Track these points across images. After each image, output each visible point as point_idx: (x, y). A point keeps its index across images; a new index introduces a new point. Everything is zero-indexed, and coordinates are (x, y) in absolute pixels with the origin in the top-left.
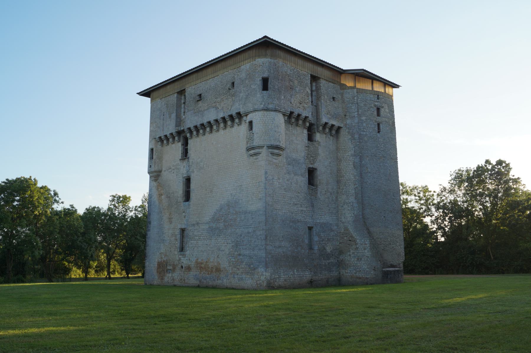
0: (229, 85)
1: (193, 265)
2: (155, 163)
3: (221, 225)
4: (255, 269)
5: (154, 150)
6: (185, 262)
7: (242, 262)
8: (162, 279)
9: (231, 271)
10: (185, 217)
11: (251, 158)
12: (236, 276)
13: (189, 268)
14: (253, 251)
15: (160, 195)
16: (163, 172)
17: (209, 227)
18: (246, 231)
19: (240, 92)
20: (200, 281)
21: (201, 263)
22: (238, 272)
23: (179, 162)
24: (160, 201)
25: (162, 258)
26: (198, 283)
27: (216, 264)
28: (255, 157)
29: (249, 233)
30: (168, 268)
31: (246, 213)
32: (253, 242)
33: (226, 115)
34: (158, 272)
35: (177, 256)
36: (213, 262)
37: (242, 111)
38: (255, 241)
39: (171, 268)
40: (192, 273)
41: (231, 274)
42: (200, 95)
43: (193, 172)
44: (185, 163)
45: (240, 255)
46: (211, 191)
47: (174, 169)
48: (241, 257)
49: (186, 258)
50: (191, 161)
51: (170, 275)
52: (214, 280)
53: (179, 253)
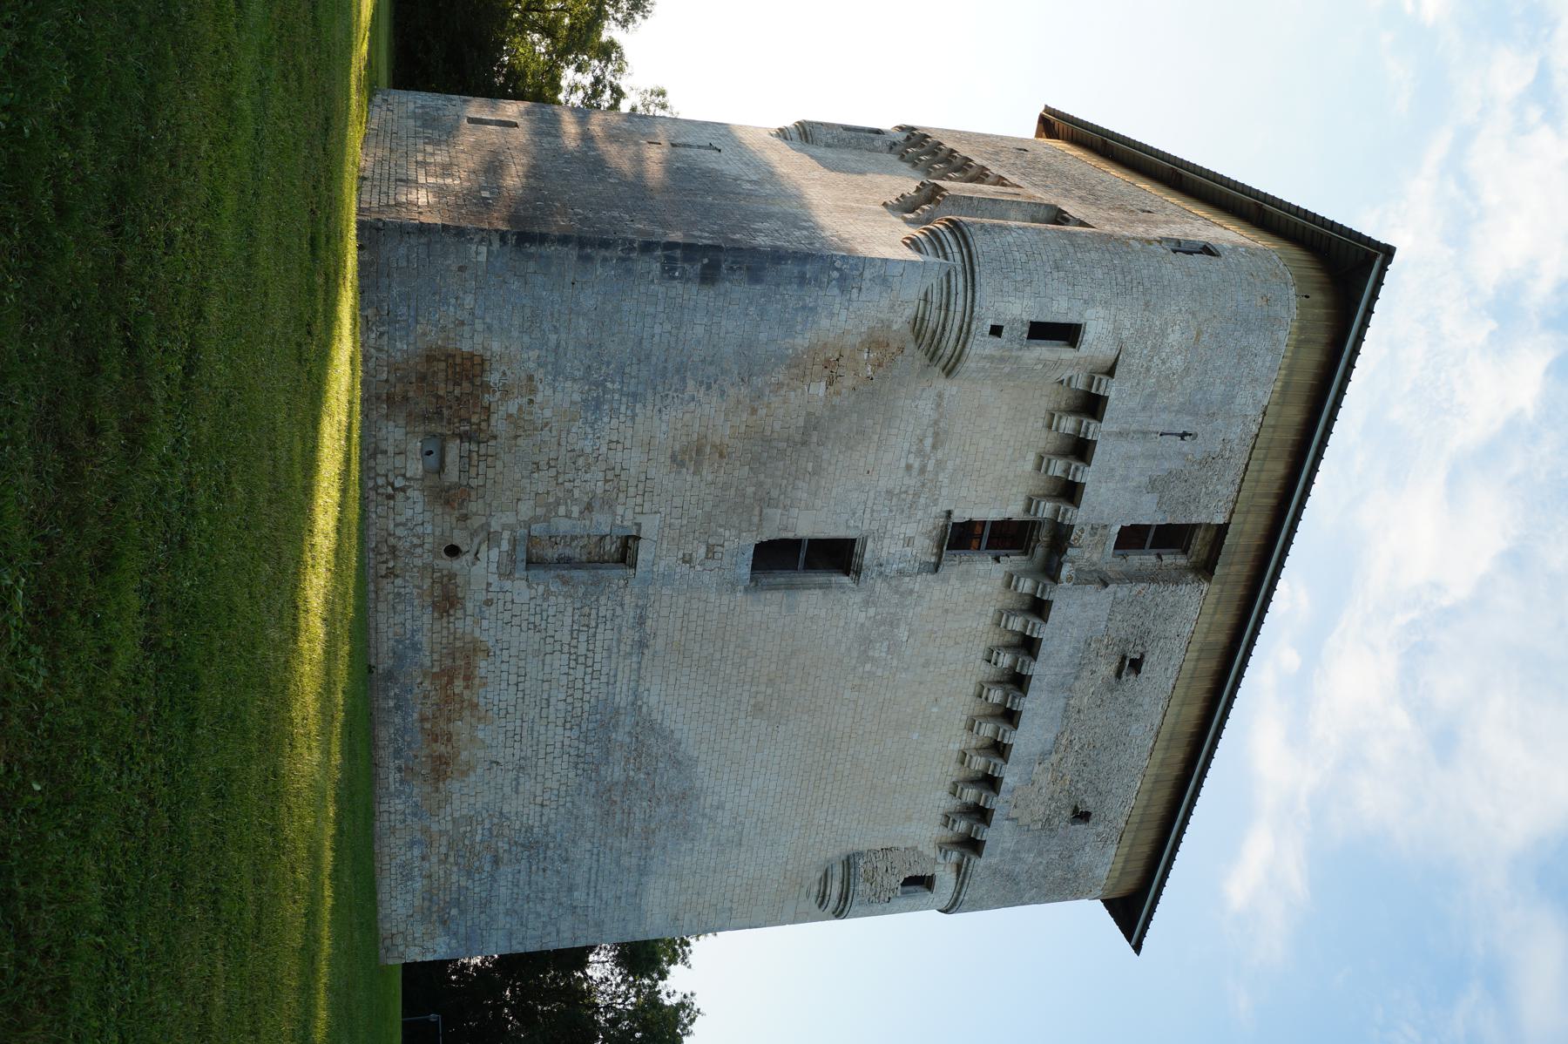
0: (1090, 803)
1: (463, 625)
2: (1002, 360)
3: (615, 773)
4: (444, 922)
5: (1066, 353)
6: (481, 572)
7: (469, 874)
8: (390, 399)
9: (435, 827)
10: (687, 560)
11: (819, 875)
12: (416, 852)
13: (447, 601)
14: (507, 913)
15: (831, 369)
16: (941, 383)
17: (617, 711)
18: (578, 880)
19: (1040, 854)
20: (390, 676)
21: (467, 678)
22: (434, 859)
23: (945, 506)
24: (799, 368)
25: (506, 392)
26: (385, 663)
27: (464, 755)
28: (816, 889)
29: (570, 889)
30: (453, 450)
31: (643, 871)
32: (539, 908)
33: (999, 804)
34: (430, 358)
35: (509, 518)
36: (473, 739)
37: (979, 864)
38: (538, 915)
39: (452, 474)
40: (427, 618)
41: (426, 831)
42: (1136, 665)
43: (867, 603)
44: (924, 547)
45: (496, 861)
46: (758, 709)
47: (922, 470)
48: (487, 868)
49: (493, 579)
50: (918, 583)
51: (415, 468)
52: (398, 753)
53: (522, 532)
